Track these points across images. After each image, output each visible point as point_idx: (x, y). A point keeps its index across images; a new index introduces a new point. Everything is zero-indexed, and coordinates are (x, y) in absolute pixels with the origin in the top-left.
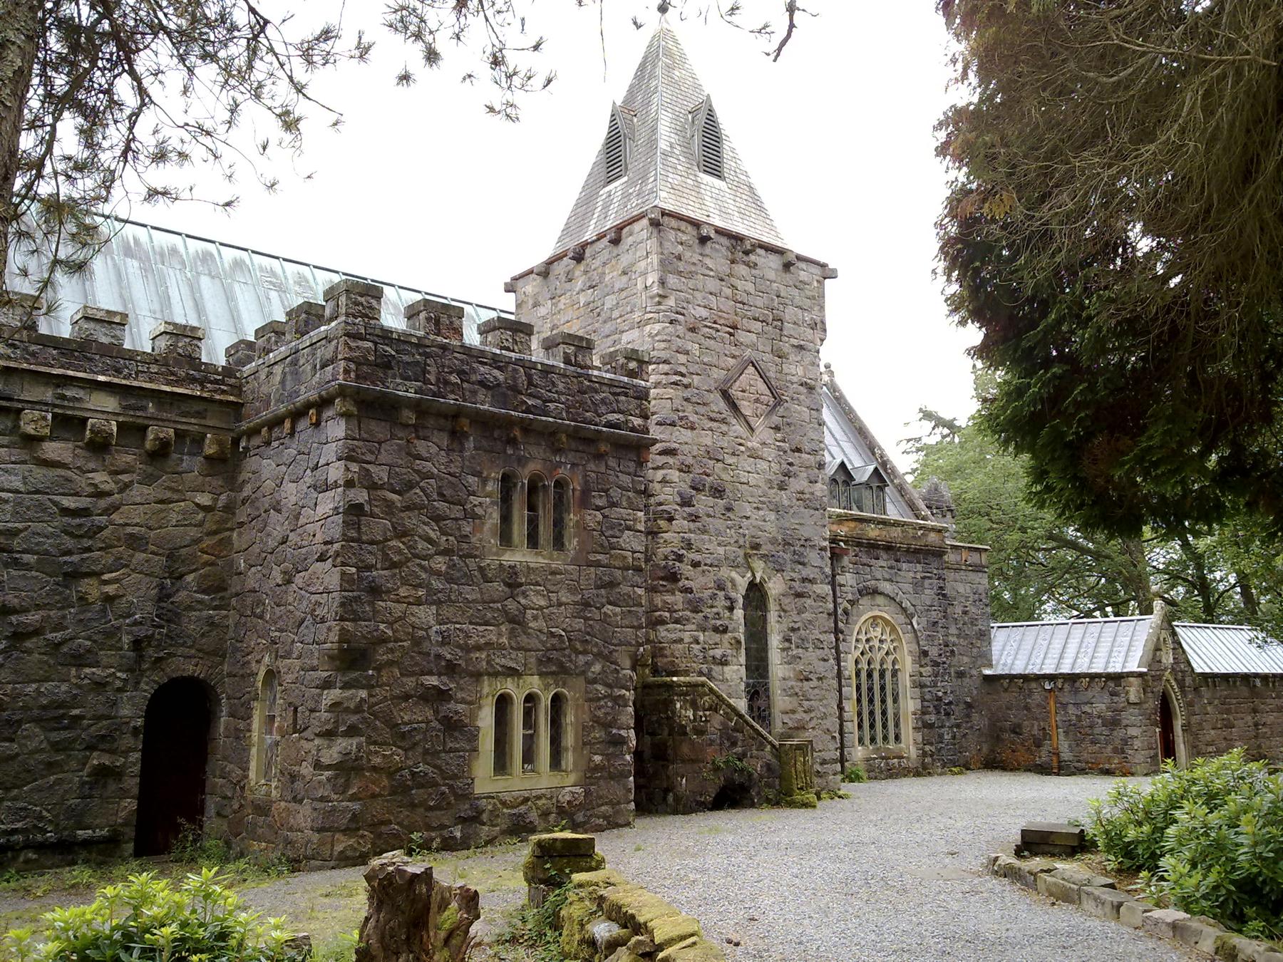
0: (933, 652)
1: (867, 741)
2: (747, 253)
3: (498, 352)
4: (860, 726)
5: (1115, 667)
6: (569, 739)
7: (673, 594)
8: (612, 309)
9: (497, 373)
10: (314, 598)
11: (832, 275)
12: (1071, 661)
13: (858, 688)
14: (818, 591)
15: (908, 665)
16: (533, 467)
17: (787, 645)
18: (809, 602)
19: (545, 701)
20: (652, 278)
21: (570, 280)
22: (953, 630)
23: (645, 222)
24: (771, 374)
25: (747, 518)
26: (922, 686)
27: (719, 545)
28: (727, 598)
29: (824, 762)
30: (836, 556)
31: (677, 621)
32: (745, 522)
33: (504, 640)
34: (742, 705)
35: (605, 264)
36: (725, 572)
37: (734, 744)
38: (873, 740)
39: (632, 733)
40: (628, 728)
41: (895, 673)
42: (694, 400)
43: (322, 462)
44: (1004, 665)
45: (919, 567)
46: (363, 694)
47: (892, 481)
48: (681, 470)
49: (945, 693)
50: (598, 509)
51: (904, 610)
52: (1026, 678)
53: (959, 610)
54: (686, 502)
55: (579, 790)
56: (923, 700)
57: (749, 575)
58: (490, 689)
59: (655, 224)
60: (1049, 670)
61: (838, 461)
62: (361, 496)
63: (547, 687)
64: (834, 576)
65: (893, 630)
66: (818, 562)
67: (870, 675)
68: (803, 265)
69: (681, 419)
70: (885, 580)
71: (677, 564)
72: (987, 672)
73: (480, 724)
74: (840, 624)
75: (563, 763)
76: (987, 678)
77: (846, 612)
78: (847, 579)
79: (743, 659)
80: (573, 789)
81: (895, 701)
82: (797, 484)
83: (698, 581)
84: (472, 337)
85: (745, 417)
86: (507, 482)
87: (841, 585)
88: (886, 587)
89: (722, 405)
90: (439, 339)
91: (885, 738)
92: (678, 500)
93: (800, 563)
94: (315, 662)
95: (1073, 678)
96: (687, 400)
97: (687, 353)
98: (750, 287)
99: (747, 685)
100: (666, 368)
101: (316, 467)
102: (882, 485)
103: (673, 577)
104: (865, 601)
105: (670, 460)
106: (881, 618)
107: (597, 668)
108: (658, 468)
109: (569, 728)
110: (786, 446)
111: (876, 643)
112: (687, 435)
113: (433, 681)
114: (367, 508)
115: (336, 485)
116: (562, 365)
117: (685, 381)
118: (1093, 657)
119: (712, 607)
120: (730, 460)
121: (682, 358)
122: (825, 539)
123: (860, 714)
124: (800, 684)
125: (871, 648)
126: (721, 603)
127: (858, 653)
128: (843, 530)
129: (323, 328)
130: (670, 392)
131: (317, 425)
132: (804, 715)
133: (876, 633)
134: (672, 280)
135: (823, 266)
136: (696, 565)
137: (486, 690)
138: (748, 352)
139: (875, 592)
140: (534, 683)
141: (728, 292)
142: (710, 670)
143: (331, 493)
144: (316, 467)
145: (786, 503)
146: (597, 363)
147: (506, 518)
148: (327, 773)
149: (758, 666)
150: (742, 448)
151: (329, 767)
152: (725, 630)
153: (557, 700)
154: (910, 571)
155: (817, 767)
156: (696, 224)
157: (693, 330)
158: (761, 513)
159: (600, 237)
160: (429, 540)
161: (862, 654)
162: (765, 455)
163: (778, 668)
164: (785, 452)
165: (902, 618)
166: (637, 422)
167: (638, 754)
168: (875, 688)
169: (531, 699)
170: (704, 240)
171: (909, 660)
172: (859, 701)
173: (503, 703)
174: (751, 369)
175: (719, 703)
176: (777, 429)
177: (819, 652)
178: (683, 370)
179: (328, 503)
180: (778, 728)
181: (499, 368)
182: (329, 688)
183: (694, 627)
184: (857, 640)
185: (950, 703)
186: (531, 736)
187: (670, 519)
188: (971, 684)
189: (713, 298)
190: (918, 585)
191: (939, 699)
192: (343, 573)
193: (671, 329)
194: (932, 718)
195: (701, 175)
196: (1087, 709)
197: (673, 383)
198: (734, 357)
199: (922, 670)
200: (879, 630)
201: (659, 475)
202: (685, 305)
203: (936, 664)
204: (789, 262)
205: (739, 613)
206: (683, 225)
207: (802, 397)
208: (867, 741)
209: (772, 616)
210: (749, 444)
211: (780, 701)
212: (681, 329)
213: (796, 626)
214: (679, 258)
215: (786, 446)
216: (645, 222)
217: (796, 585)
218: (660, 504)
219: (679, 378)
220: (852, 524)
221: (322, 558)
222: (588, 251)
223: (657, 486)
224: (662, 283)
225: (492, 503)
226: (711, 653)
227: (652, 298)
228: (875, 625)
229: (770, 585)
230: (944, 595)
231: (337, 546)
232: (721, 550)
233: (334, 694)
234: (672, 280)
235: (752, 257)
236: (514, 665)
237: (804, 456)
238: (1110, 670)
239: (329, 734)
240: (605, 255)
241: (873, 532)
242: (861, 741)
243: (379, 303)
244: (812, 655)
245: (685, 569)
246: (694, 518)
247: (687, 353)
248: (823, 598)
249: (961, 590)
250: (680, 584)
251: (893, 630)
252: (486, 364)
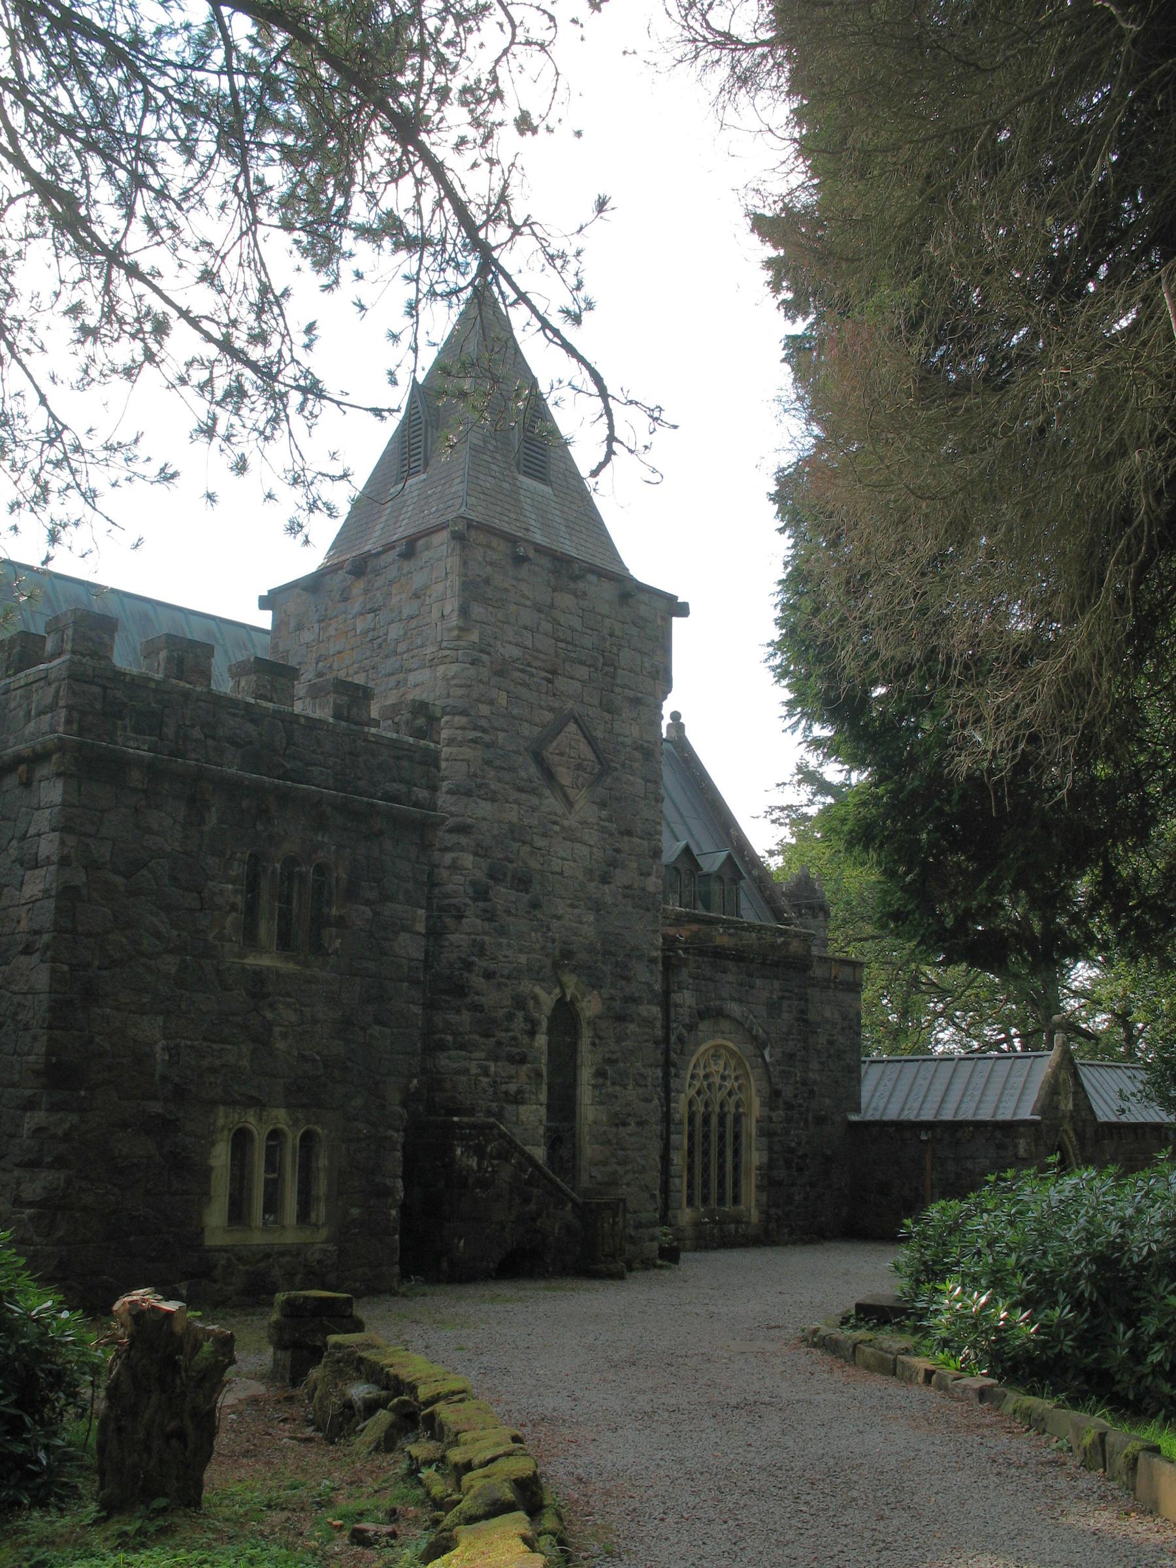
0: (788, 1092)
1: (698, 1201)
2: (575, 578)
3: (252, 701)
4: (690, 1185)
5: (1005, 1115)
6: (321, 1187)
7: (458, 1012)
8: (397, 641)
9: (250, 727)
10: (17, 999)
11: (682, 610)
12: (955, 1106)
13: (691, 1137)
14: (645, 1014)
15: (756, 1108)
17: (601, 1081)
18: (632, 1027)
19: (293, 1139)
20: (451, 606)
21: (345, 600)
22: (814, 1065)
23: (444, 535)
24: (599, 734)
25: (559, 918)
27: (521, 951)
28: (528, 1019)
29: (639, 1225)
30: (669, 966)
31: (462, 1047)
32: (555, 924)
33: (245, 1063)
34: (539, 1153)
35: (391, 583)
36: (526, 986)
37: (526, 1201)
38: (705, 1200)
39: (399, 1183)
40: (396, 1177)
41: (738, 1119)
42: (497, 763)
43: (32, 831)
44: (875, 1109)
45: (776, 984)
46: (74, 1118)
47: (750, 873)
48: (476, 854)
49: (799, 1144)
50: (368, 903)
51: (755, 1038)
52: (900, 1126)
53: (823, 1040)
54: (481, 893)
55: (331, 1247)
56: (770, 1149)
57: (557, 990)
58: (224, 1118)
59: (458, 537)
60: (928, 1115)
61: (682, 844)
62: (79, 878)
63: (296, 1123)
64: (667, 992)
65: (740, 1064)
66: (647, 977)
67: (706, 1120)
68: (644, 597)
69: (479, 786)
70: (735, 1000)
71: (466, 974)
72: (854, 1118)
73: (214, 1162)
74: (673, 1056)
75: (313, 1216)
77: (680, 1039)
78: (686, 998)
79: (543, 1097)
80: (325, 1246)
81: (736, 1152)
82: (621, 877)
83: (493, 998)
84: (223, 684)
85: (562, 787)
87: (676, 1005)
88: (734, 1008)
89: (533, 770)
90: (182, 684)
91: (721, 1200)
92: (470, 890)
93: (623, 978)
94: (17, 1077)
95: (954, 1126)
96: (488, 762)
97: (491, 703)
98: (577, 623)
99: (548, 1129)
100: (461, 720)
101: (24, 837)
102: (737, 876)
103: (460, 990)
104: (704, 1026)
105: (463, 840)
106: (725, 1047)
107: (358, 1102)
108: (445, 850)
109: (322, 1175)
110: (613, 827)
111: (717, 1080)
112: (485, 809)
113: (156, 1107)
114: (84, 892)
115: (48, 861)
116: (331, 720)
117: (487, 738)
118: (980, 1101)
119: (507, 1030)
120: (540, 842)
121: (485, 710)
122: (656, 949)
123: (690, 1169)
124: (614, 1130)
125: (709, 1086)
126: (519, 1024)
127: (693, 1092)
128: (683, 933)
129: (42, 667)
130: (467, 752)
131: (27, 784)
132: (618, 1168)
133: (717, 1068)
134: (477, 611)
135: (671, 599)
136: (489, 975)
137: (221, 1122)
138: (570, 704)
139: (719, 1014)
140: (280, 1117)
141: (547, 626)
142: (502, 1109)
143: (43, 872)
144: (24, 837)
145: (609, 900)
146: (374, 714)
147: (252, 909)
148: (29, 1211)
149: (563, 1105)
150: (557, 828)
151: (30, 1204)
152: (523, 1060)
153: (308, 1138)
154: (765, 989)
155: (631, 1231)
156: (513, 540)
157: (499, 673)
158: (576, 911)
159: (389, 548)
160: (158, 935)
161: (699, 1093)
162: (586, 838)
163: (589, 1110)
164: (611, 835)
165: (750, 1049)
166: (422, 794)
167: (404, 1208)
168: (716, 1134)
169: (275, 1135)
170: (519, 560)
171: (756, 1102)
172: (691, 1152)
173: (241, 1139)
174: (572, 727)
175: (510, 1149)
176: (603, 805)
177: (641, 1090)
178: (484, 723)
179: (36, 884)
180: (584, 1182)
181: (252, 721)
182: (33, 1109)
183: (482, 1055)
184: (693, 1077)
185: (805, 1156)
186: (275, 1181)
187: (460, 917)
189: (528, 634)
190: (773, 1008)
191: (792, 1151)
192: (53, 971)
193: (472, 672)
194: (780, 1174)
195: (522, 478)
196: (969, 1165)
197: (472, 741)
198: (552, 710)
199: (773, 1114)
200: (722, 1063)
201: (448, 858)
202: (492, 641)
203: (789, 1106)
204: (630, 591)
205: (542, 1040)
206: (495, 542)
207: (636, 765)
208: (698, 1201)
209: (585, 1045)
210: (566, 823)
211: (589, 1150)
212: (485, 672)
213: (614, 1057)
214: (487, 581)
215: (613, 827)
216: (444, 535)
217: (617, 1004)
218: (447, 896)
219: (480, 734)
220: (695, 927)
221: (28, 950)
223: (445, 874)
224: (464, 612)
225: (236, 892)
226: (504, 1087)
227: (450, 630)
228: (716, 1056)
229: (584, 1004)
230: (806, 1021)
231: (46, 938)
232: (523, 959)
233: (39, 1117)
234: (477, 611)
235: (581, 585)
236: (255, 1094)
237: (636, 840)
238: (1000, 1117)
239: (32, 1165)
240: (392, 573)
241: (722, 938)
242: (690, 1202)
243: (112, 637)
244: (632, 1093)
245: (477, 981)
246: (489, 916)
247: (491, 703)
248: (648, 1023)
249: (828, 1014)
250: (468, 1000)
251: (740, 1064)
252: (235, 715)
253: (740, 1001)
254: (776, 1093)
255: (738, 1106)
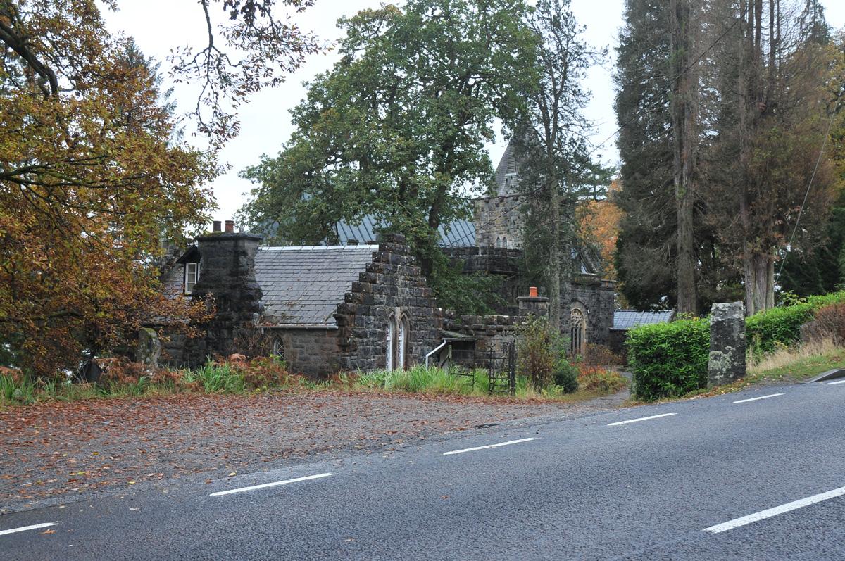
0: (594, 322)
15: (585, 326)
16: (518, 284)
18: (565, 310)
26: (589, 334)
51: (586, 306)
65: (581, 314)
72: (611, 329)
76: (611, 331)
81: (580, 339)
86: (514, 287)
88: (580, 299)
165: (584, 310)
171: (585, 325)
188: (605, 333)
222: (505, 200)
253: (581, 296)
254: (591, 322)
255: (581, 325)
